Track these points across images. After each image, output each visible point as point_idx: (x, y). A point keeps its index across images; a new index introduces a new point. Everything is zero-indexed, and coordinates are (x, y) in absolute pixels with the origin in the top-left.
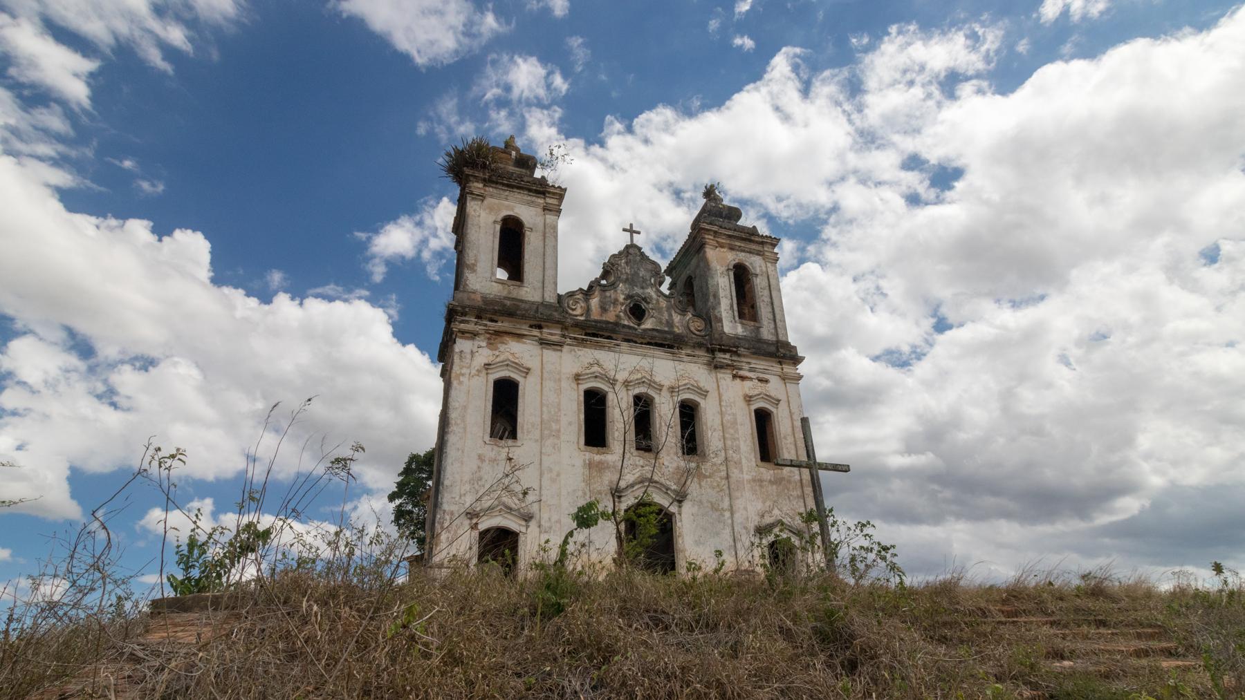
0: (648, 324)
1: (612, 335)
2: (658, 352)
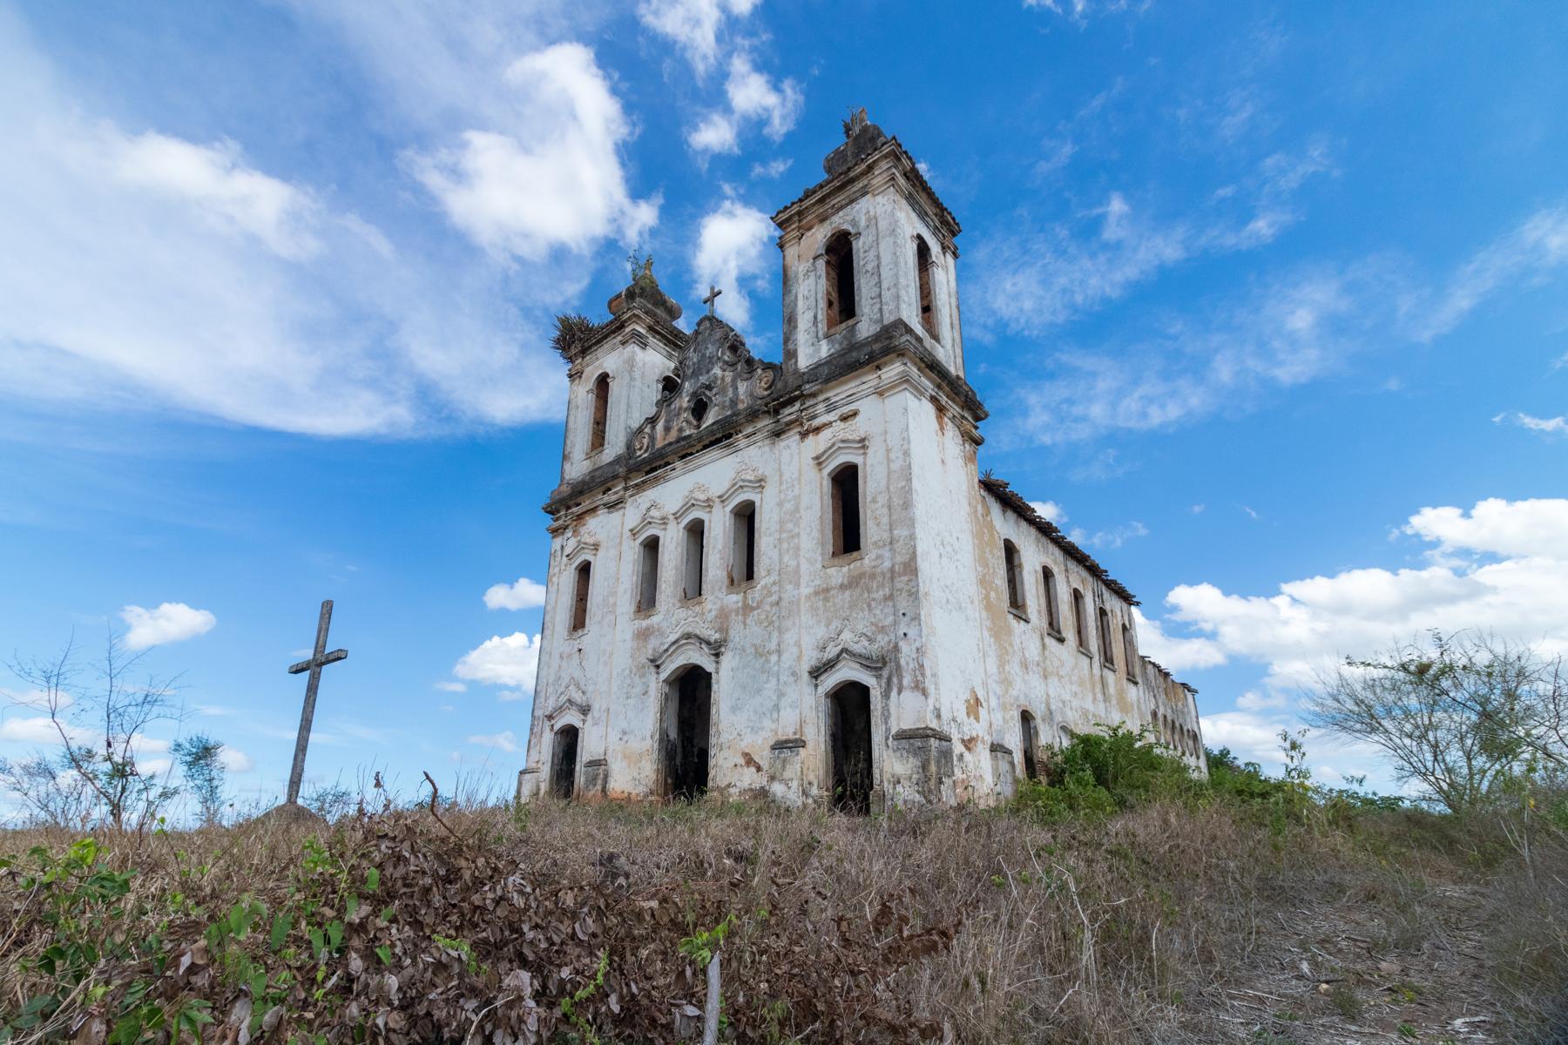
0: (710, 418)
1: (666, 460)
2: (714, 453)
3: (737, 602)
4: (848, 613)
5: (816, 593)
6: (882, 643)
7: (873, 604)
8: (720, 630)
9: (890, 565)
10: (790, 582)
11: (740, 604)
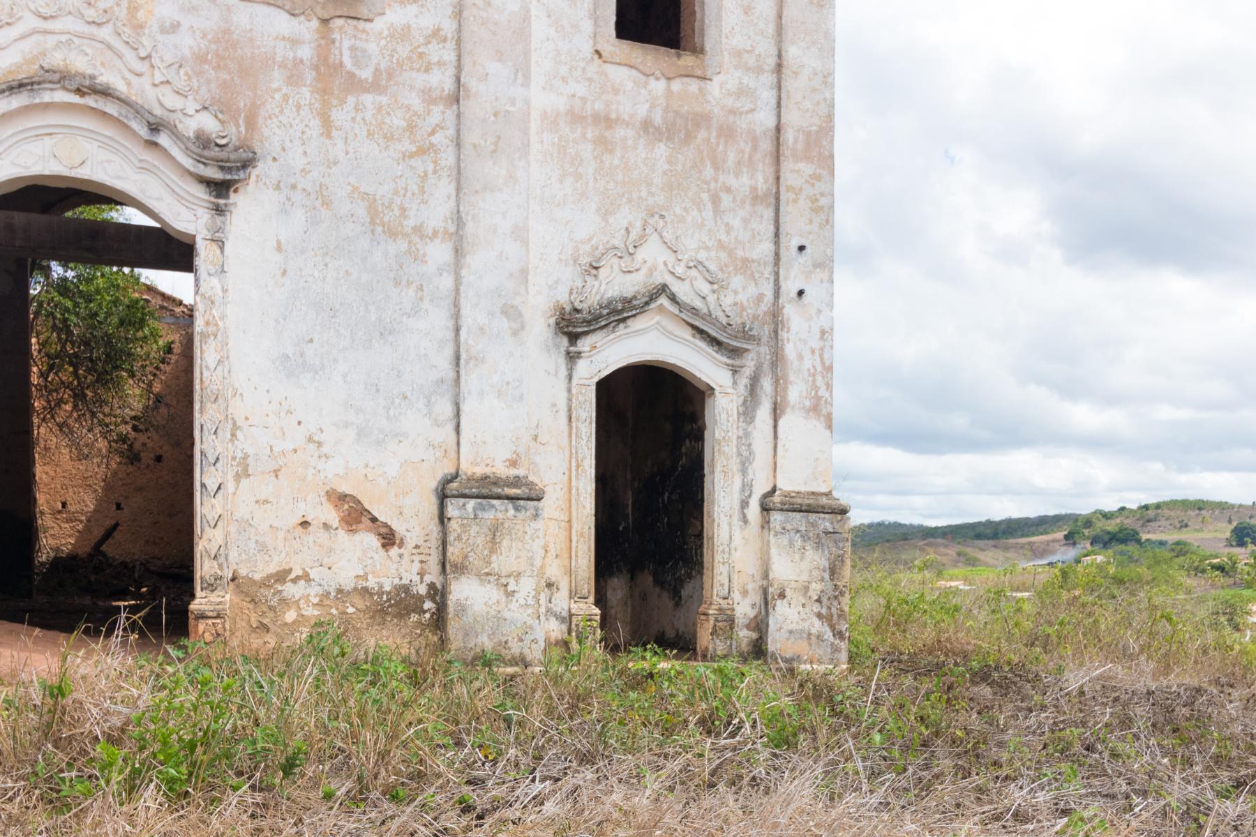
3: (295, 42)
4: (661, 199)
5: (576, 118)
6: (742, 298)
7: (726, 200)
8: (220, 107)
9: (771, 122)
10: (500, 56)
11: (306, 52)
